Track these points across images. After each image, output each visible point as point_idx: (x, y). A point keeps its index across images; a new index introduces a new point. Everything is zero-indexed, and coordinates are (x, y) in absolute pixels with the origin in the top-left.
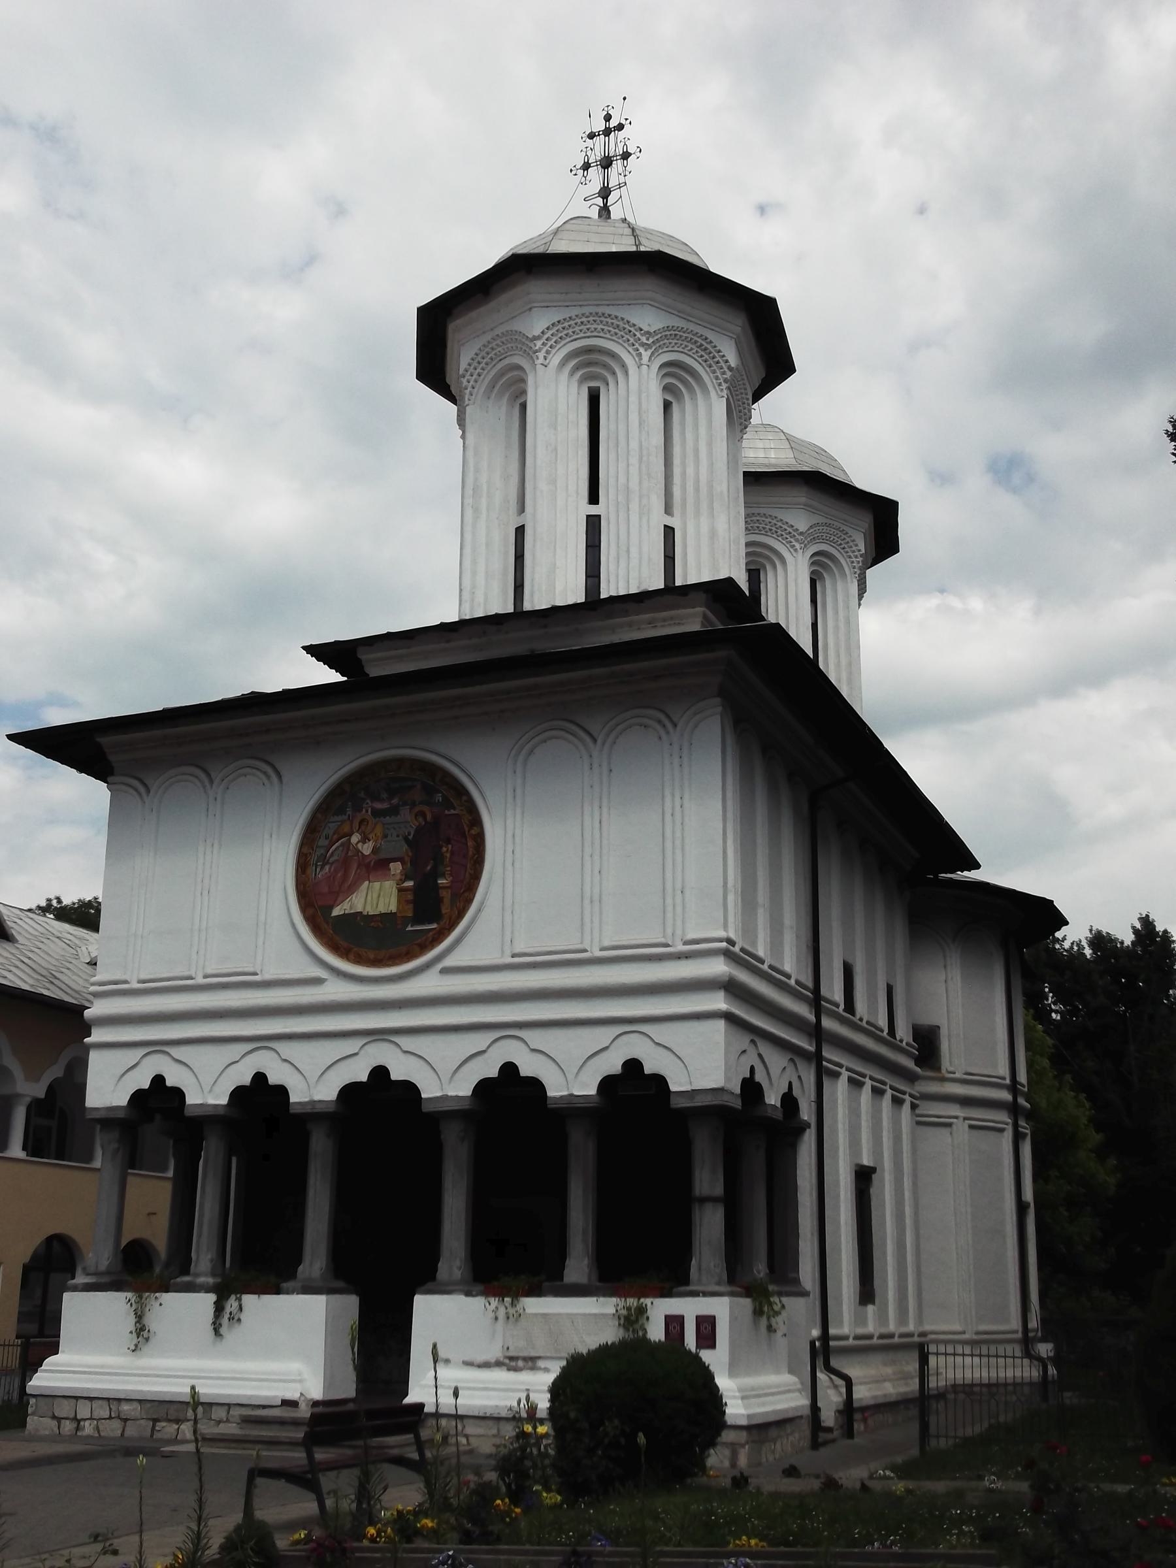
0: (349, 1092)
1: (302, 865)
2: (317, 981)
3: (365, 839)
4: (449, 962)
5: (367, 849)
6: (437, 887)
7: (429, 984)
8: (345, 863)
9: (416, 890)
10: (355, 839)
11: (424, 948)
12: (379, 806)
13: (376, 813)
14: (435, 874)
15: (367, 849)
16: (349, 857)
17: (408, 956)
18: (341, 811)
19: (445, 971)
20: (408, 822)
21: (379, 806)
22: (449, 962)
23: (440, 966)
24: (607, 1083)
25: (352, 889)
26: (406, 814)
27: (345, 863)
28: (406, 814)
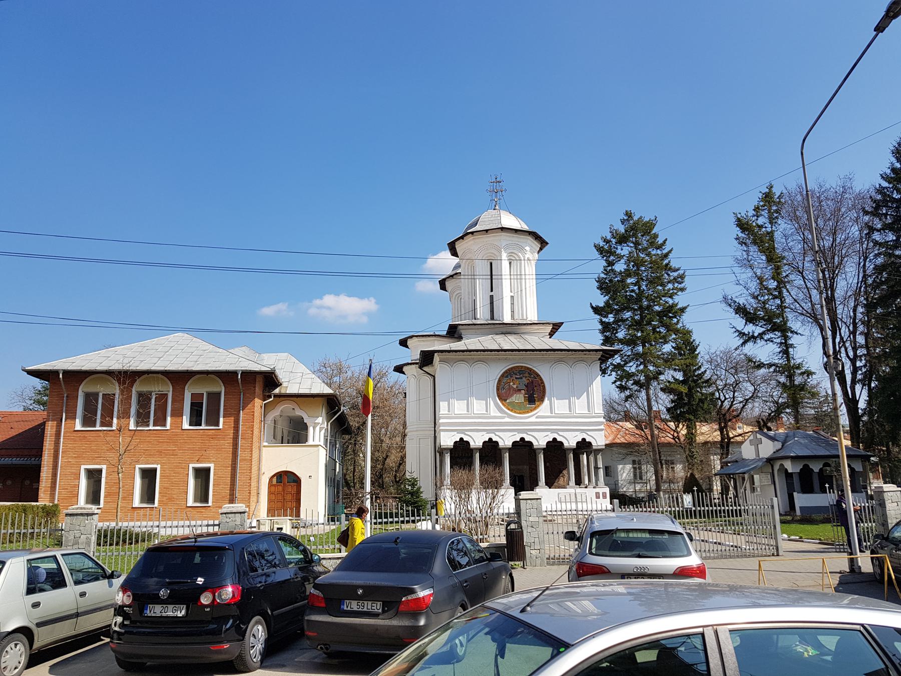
0: (514, 443)
1: (498, 389)
2: (503, 418)
3: (514, 384)
4: (538, 414)
5: (515, 386)
6: (534, 397)
7: (533, 419)
8: (509, 389)
9: (528, 397)
10: (511, 384)
11: (532, 411)
12: (517, 376)
13: (516, 378)
14: (533, 394)
15: (515, 386)
16: (510, 388)
17: (528, 412)
18: (507, 377)
19: (537, 418)
20: (525, 381)
21: (517, 376)
22: (538, 414)
23: (536, 415)
24: (578, 443)
25: (512, 395)
26: (524, 379)
27: (509, 389)
28: (524, 379)
